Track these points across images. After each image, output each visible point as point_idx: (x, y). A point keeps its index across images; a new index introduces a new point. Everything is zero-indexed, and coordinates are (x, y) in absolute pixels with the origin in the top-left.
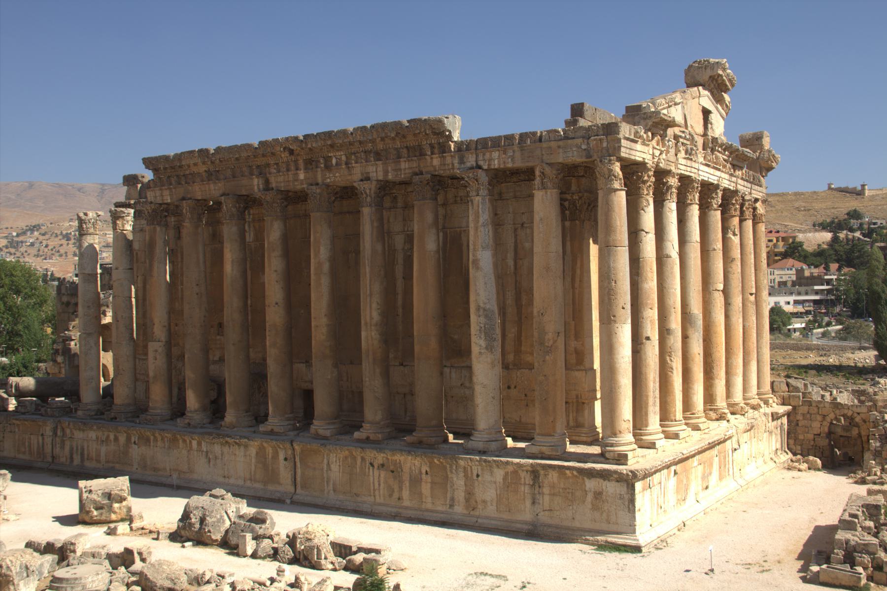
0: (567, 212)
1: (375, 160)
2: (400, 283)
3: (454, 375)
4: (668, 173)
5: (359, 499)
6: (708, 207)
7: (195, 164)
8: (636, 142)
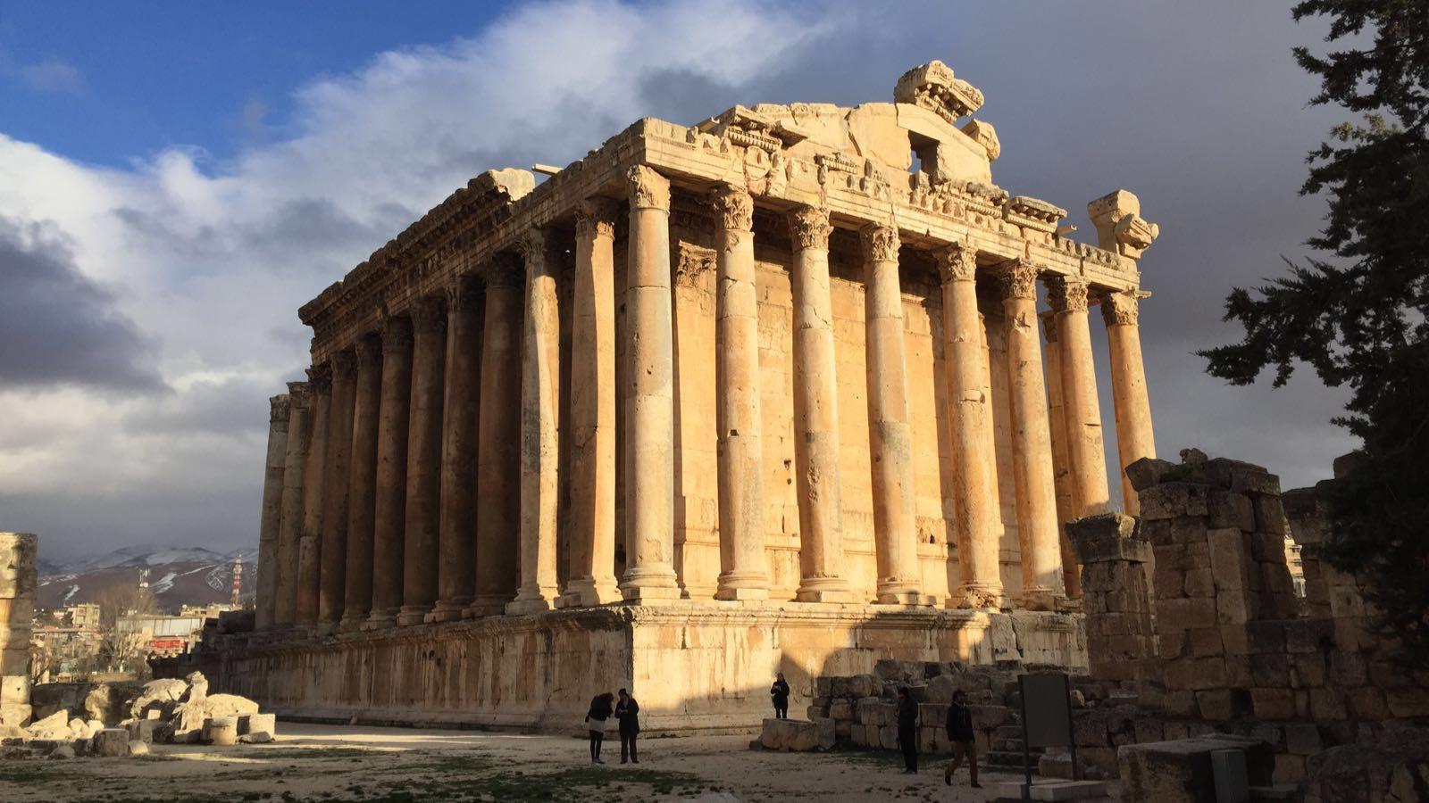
4: (804, 208)
6: (949, 280)
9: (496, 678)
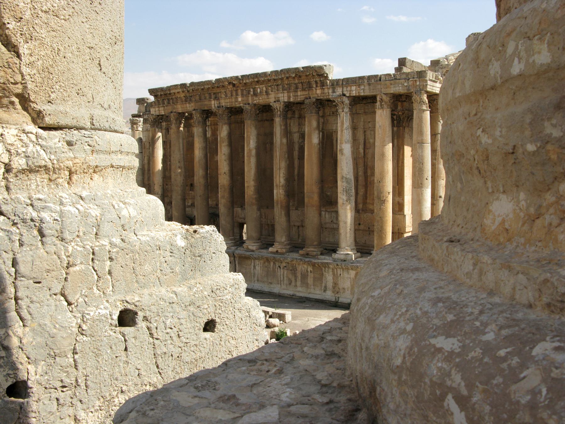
0: (395, 122)
1: (283, 90)
2: (296, 162)
3: (327, 216)
5: (272, 286)
7: (178, 93)
8: (436, 82)
9: (335, 284)
